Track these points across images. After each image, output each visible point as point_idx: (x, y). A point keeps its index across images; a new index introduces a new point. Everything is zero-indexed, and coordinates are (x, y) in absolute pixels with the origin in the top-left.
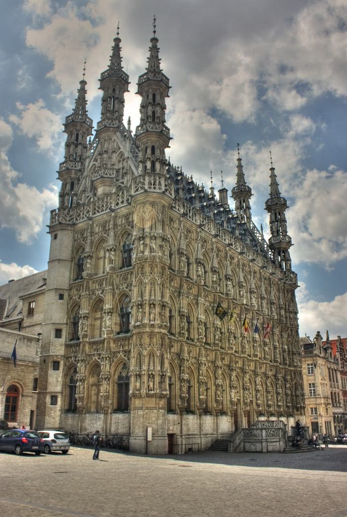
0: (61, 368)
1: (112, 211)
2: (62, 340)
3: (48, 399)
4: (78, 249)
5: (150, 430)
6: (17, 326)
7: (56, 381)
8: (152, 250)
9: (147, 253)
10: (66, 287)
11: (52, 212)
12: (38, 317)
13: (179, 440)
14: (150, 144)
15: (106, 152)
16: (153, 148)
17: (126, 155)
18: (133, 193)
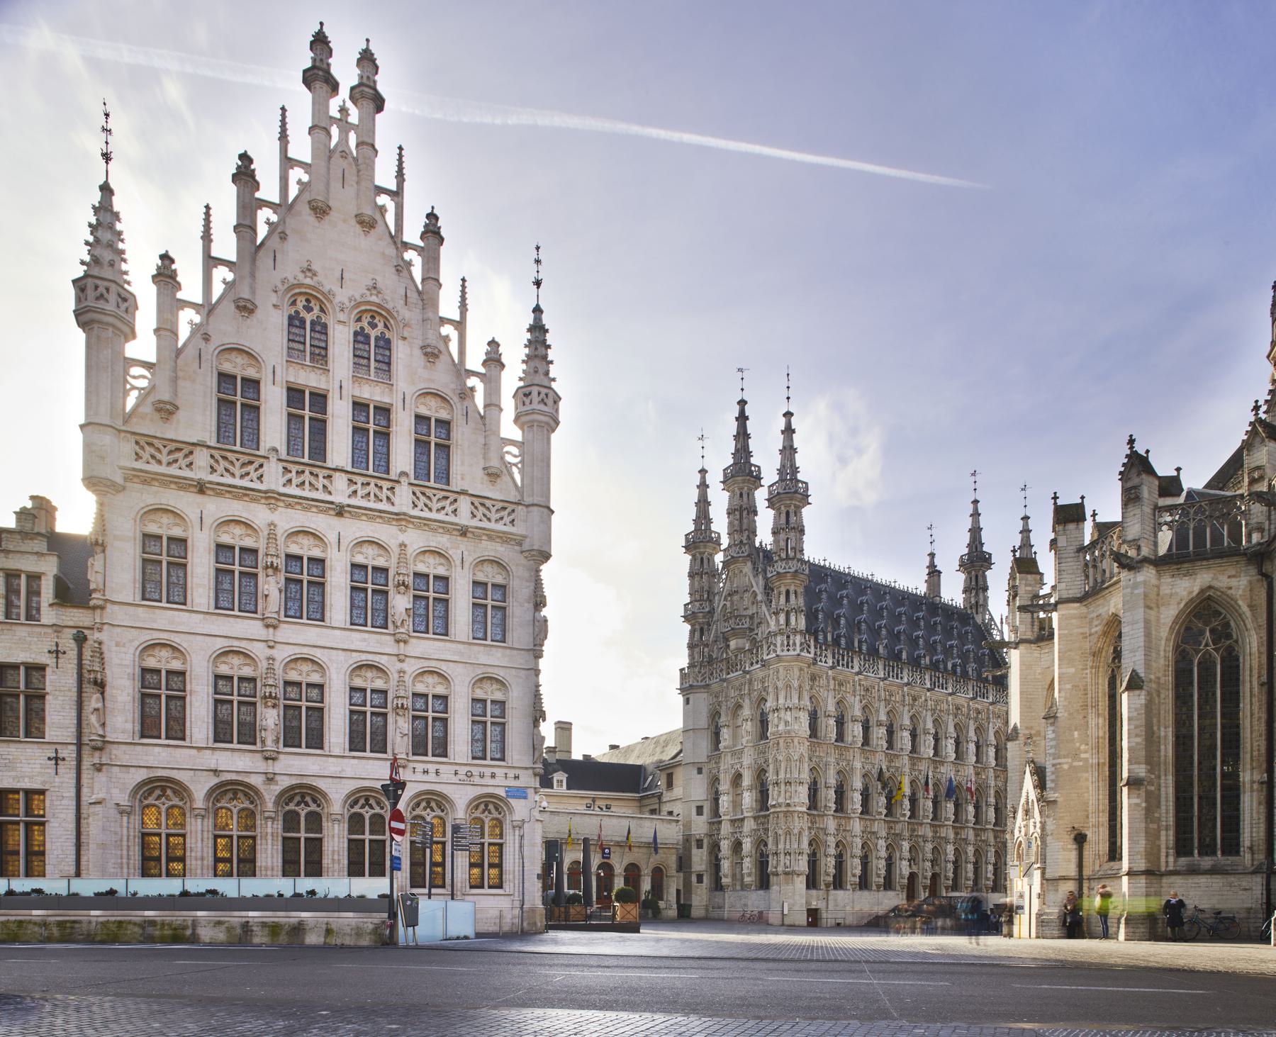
0: (705, 846)
1: (746, 672)
2: (704, 818)
3: (694, 879)
4: (715, 715)
5: (786, 905)
6: (656, 800)
7: (699, 859)
8: (786, 723)
9: (781, 727)
10: (704, 759)
11: (682, 670)
12: (678, 791)
13: (824, 915)
14: (783, 589)
15: (736, 592)
16: (788, 592)
17: (759, 598)
18: (765, 657)
